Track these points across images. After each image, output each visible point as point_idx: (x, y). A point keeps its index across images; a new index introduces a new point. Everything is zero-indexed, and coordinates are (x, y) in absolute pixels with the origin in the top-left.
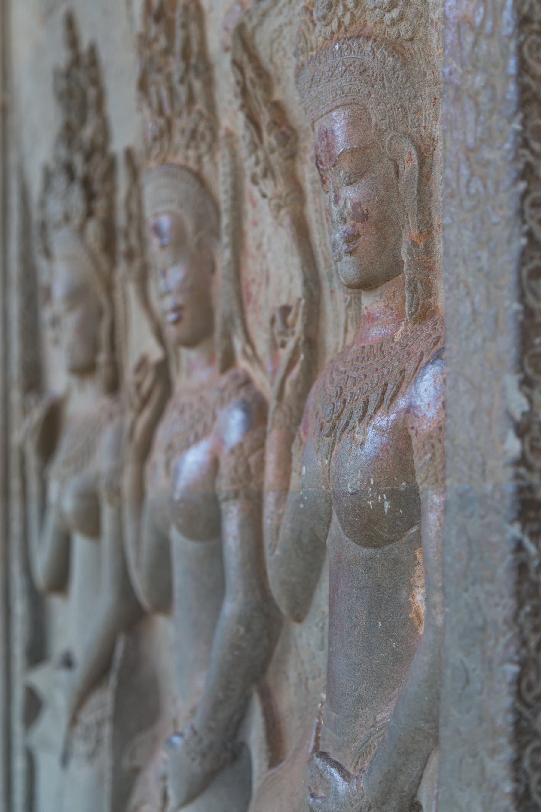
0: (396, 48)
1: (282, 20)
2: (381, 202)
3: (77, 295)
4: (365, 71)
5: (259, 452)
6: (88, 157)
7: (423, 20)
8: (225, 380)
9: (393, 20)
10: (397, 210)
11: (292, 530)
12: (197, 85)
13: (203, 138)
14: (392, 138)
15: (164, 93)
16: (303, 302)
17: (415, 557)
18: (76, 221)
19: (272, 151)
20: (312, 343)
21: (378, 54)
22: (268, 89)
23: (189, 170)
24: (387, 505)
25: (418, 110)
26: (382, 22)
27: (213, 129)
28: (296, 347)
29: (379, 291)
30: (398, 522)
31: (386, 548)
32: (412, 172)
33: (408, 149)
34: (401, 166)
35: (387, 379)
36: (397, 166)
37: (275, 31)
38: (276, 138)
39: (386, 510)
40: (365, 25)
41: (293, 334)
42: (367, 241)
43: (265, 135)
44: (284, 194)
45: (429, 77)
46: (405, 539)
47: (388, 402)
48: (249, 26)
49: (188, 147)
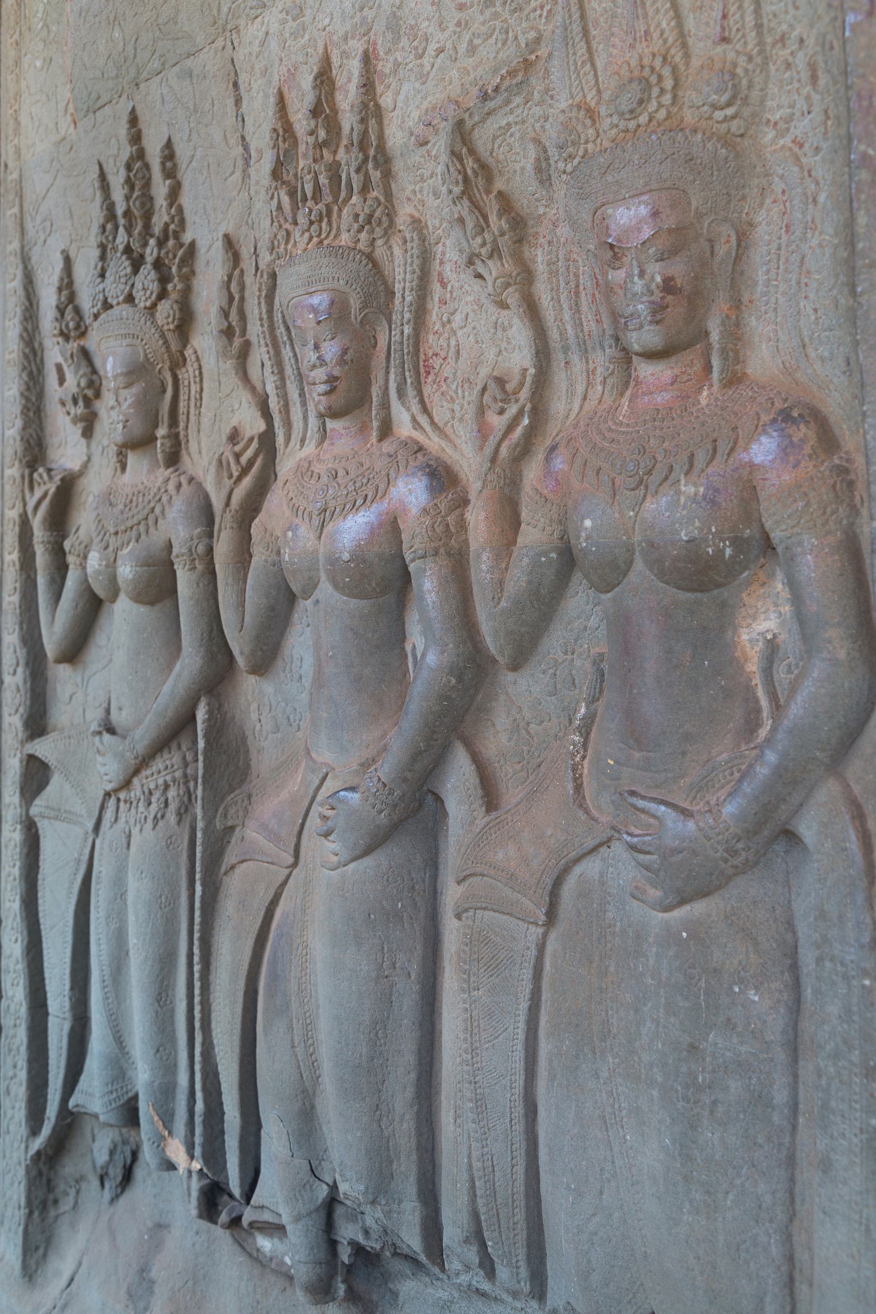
0: (727, 140)
1: (511, 118)
2: (696, 278)
3: (137, 371)
4: (691, 160)
5: (457, 512)
6: (161, 244)
7: (757, 120)
8: (388, 446)
9: (726, 116)
10: (709, 286)
11: (529, 582)
12: (376, 175)
13: (379, 224)
14: (712, 221)
15: (323, 180)
16: (532, 371)
17: (741, 599)
18: (142, 300)
19: (502, 234)
20: (538, 410)
21: (709, 146)
22: (489, 179)
23: (360, 251)
24: (728, 552)
25: (744, 198)
26: (710, 118)
27: (391, 215)
28: (520, 413)
29: (673, 359)
30: (737, 567)
31: (715, 592)
32: (728, 253)
33: (727, 232)
34: (717, 247)
35: (715, 435)
36: (712, 247)
37: (500, 128)
38: (508, 222)
39: (727, 556)
40: (682, 121)
41: (517, 401)
42: (676, 311)
43: (493, 218)
44: (514, 274)
45: (758, 169)
46: (737, 582)
47: (725, 457)
48: (469, 123)
49: (360, 230)
